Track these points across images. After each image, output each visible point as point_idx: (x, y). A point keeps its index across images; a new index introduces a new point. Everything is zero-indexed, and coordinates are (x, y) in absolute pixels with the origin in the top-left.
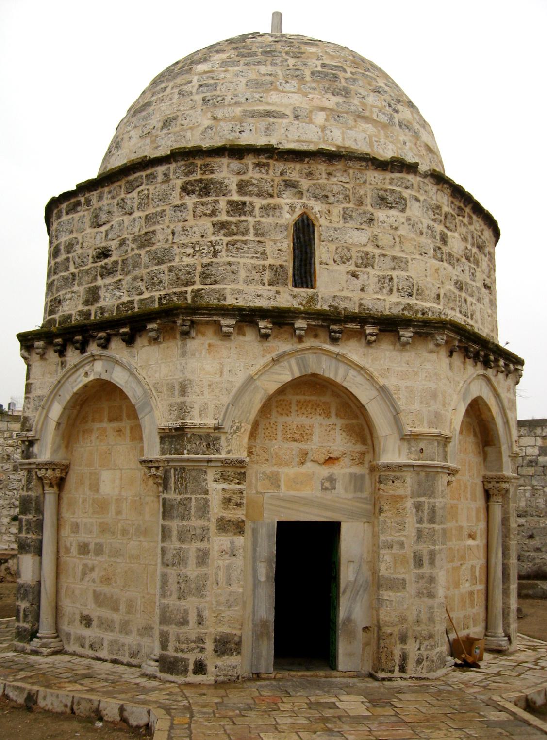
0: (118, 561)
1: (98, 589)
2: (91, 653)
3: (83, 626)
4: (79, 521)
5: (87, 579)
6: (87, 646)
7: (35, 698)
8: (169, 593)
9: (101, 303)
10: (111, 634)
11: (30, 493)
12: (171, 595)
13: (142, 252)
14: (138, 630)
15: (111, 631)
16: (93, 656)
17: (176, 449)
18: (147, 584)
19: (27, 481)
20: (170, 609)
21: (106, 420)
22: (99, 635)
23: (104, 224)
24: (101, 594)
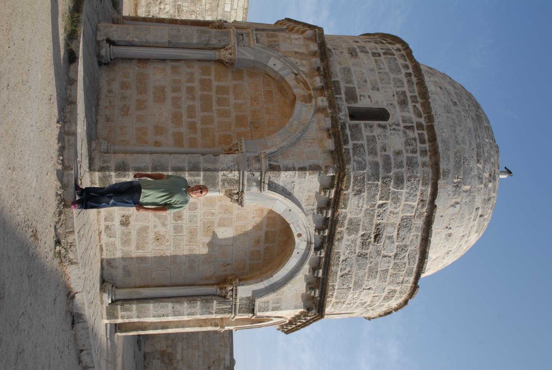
0: (172, 247)
1: (150, 231)
2: (102, 228)
3: (121, 218)
4: (198, 210)
5: (156, 220)
6: (107, 223)
7: (81, 320)
8: (156, 309)
9: (346, 236)
10: (120, 245)
11: (220, 183)
12: (155, 311)
13: (367, 270)
14: (127, 266)
15: (122, 244)
16: (101, 229)
17: (242, 308)
18: (158, 271)
19: (230, 180)
20: (147, 311)
21: (268, 229)
22: (117, 233)
23: (398, 234)
24: (147, 233)
